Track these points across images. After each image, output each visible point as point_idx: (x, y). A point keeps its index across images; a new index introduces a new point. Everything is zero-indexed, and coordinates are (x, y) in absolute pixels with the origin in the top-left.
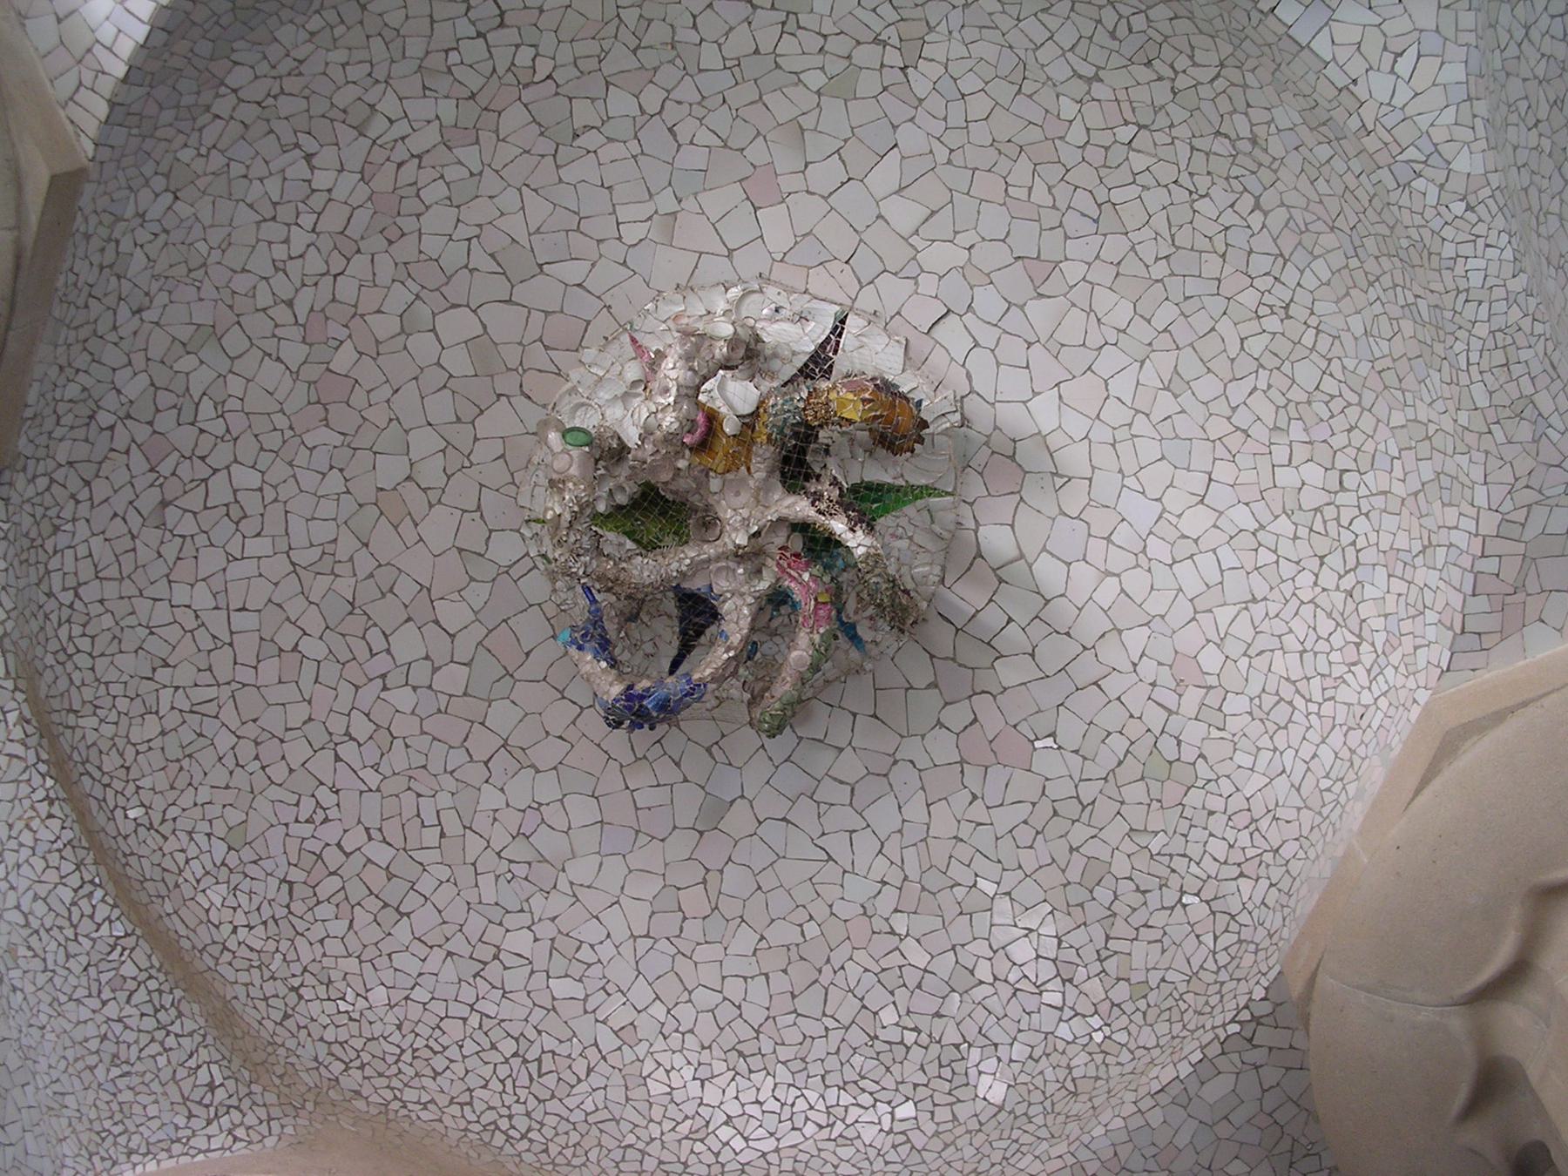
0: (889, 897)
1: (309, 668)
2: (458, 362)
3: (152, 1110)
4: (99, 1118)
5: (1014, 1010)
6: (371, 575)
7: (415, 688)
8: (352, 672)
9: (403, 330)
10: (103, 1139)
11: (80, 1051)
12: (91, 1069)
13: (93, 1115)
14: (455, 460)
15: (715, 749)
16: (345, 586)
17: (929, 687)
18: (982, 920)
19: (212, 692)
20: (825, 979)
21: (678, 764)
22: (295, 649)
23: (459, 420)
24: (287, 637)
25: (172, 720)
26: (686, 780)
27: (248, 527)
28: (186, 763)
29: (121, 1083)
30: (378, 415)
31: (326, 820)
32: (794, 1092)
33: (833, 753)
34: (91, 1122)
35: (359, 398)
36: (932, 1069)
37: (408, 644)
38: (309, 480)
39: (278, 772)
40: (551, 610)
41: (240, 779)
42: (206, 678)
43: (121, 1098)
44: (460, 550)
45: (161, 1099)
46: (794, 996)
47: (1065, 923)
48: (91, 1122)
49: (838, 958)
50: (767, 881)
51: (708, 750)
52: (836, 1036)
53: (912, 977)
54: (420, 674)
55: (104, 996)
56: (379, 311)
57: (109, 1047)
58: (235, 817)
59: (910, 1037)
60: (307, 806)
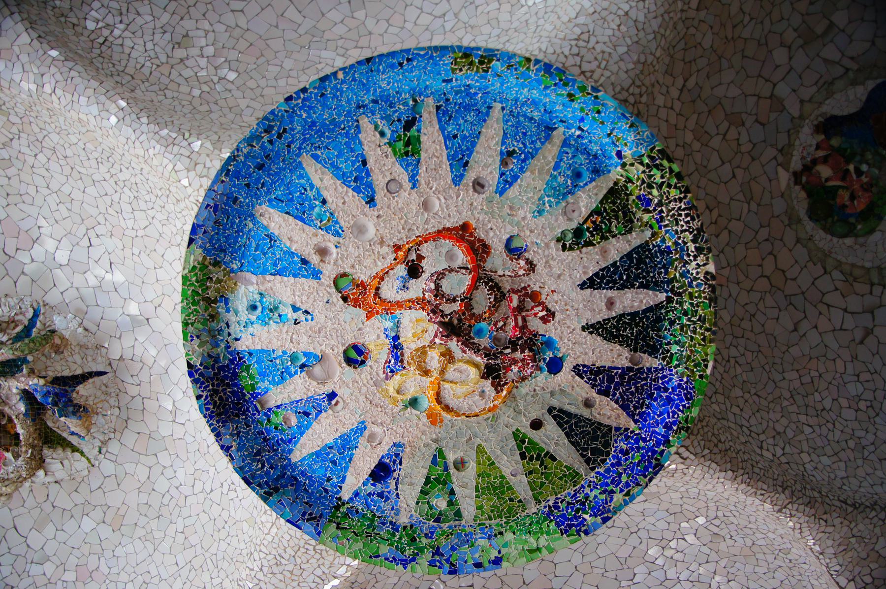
0: (100, 230)
1: (188, 522)
2: (50, 530)
3: (287, 537)
4: (313, 557)
5: (69, 153)
6: (145, 515)
7: (175, 472)
8: (181, 503)
9: (49, 560)
10: (322, 550)
11: (288, 581)
12: (291, 573)
13: (313, 561)
14: (88, 508)
15: (118, 336)
16: (154, 524)
17: (26, 275)
18: (66, 189)
19: (209, 561)
20: (141, 233)
21: (133, 346)
22: (182, 532)
23: (72, 516)
24: (180, 538)
25: (222, 575)
26: (136, 339)
27: (147, 578)
28: (234, 560)
29: (286, 556)
30: (86, 549)
31: (233, 483)
32: (179, 215)
33: (80, 290)
34: (318, 560)
35: (83, 561)
36: (117, 166)
37: (162, 485)
38: (122, 562)
39: (225, 515)
40: (118, 435)
41: (233, 533)
42: (205, 567)
43: (293, 554)
44: (119, 485)
45: (279, 536)
46: (158, 241)
47: (30, 160)
48: (318, 560)
49: (133, 233)
50: (139, 281)
51: (120, 338)
52: (151, 213)
53: (108, 200)
54: (169, 473)
55: (257, 582)
56: (44, 574)
57: (275, 569)
58: (245, 526)
59: (121, 184)
60: (232, 495)
